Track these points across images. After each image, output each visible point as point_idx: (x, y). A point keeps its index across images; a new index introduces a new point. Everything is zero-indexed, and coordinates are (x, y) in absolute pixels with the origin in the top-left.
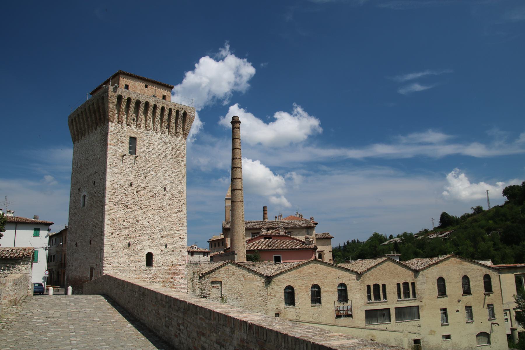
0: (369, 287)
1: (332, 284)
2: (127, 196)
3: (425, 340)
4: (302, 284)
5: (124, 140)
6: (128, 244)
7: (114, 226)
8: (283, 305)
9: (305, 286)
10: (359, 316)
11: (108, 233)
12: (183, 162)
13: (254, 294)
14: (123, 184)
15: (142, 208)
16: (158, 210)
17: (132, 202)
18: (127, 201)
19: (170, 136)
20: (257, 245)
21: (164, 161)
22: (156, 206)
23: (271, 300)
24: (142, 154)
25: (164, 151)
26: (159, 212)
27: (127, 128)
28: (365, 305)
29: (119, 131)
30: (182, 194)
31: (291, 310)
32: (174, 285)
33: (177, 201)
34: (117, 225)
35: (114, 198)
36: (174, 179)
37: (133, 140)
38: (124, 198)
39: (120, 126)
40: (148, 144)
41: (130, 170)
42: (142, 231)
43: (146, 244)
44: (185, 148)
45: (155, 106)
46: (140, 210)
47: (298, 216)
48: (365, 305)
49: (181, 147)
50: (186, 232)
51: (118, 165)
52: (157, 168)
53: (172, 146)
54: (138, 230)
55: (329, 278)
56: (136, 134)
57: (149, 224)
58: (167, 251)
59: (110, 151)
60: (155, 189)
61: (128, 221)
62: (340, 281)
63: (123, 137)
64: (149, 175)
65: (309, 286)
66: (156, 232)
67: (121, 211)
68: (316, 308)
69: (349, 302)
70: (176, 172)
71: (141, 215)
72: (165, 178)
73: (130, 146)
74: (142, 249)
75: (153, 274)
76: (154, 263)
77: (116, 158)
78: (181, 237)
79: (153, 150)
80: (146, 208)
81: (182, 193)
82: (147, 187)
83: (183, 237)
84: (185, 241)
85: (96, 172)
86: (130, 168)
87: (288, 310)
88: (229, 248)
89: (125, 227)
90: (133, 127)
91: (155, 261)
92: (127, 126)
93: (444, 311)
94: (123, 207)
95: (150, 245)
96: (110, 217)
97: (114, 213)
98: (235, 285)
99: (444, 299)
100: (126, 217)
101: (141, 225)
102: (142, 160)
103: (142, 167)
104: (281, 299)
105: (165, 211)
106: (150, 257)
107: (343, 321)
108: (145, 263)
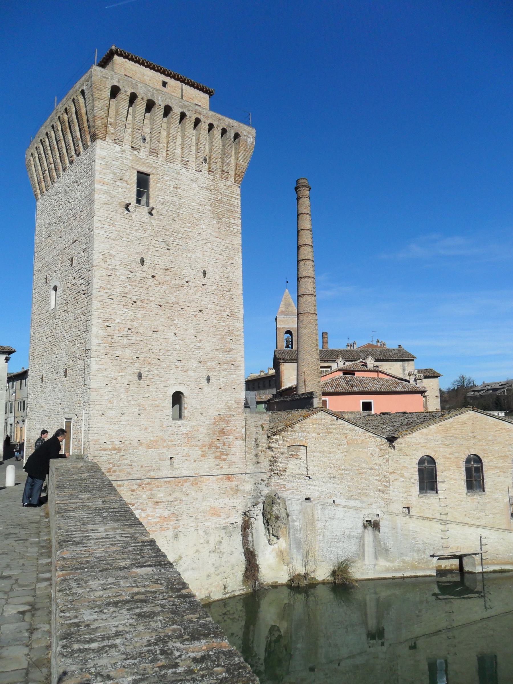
1: (503, 454)
2: (133, 284)
4: (450, 454)
5: (126, 178)
6: (137, 375)
7: (110, 339)
9: (455, 458)
11: (98, 353)
12: (234, 227)
13: (365, 470)
15: (163, 307)
16: (193, 313)
17: (144, 294)
18: (135, 293)
19: (211, 177)
20: (335, 384)
21: (201, 222)
22: (189, 304)
23: (395, 482)
24: (160, 206)
25: (200, 203)
26: (195, 316)
27: (131, 153)
29: (117, 159)
30: (234, 285)
31: (430, 498)
32: (222, 453)
33: (227, 298)
34: (115, 337)
35: (109, 286)
36: (220, 256)
38: (130, 287)
39: (118, 148)
40: (172, 189)
41: (140, 234)
42: (164, 351)
44: (239, 202)
46: (160, 311)
47: (379, 344)
49: (231, 199)
50: (243, 355)
51: (116, 223)
52: (189, 234)
53: (215, 197)
54: (155, 348)
55: (497, 443)
56: (149, 167)
57: (177, 338)
58: (210, 389)
59: (100, 196)
60: (187, 273)
61: (137, 331)
63: (124, 171)
64: (175, 247)
65: (462, 458)
66: (190, 353)
67: (123, 312)
68: (475, 499)
70: (223, 244)
71: (161, 320)
72: (205, 253)
73: (137, 190)
74: (164, 385)
75: (184, 432)
76: (185, 411)
77: (112, 210)
78: (233, 363)
79: (182, 200)
80: (170, 308)
82: (172, 269)
83: (237, 363)
85: (75, 239)
86: (140, 231)
87: (424, 501)
88: (290, 389)
89: (132, 342)
90: (143, 154)
91: (189, 408)
92: (132, 151)
94: (126, 304)
95: (178, 377)
96: (101, 321)
97: (109, 316)
98: (330, 452)
100: (132, 323)
101: (161, 340)
102: (161, 217)
103: (162, 230)
104: (413, 481)
105: (205, 314)
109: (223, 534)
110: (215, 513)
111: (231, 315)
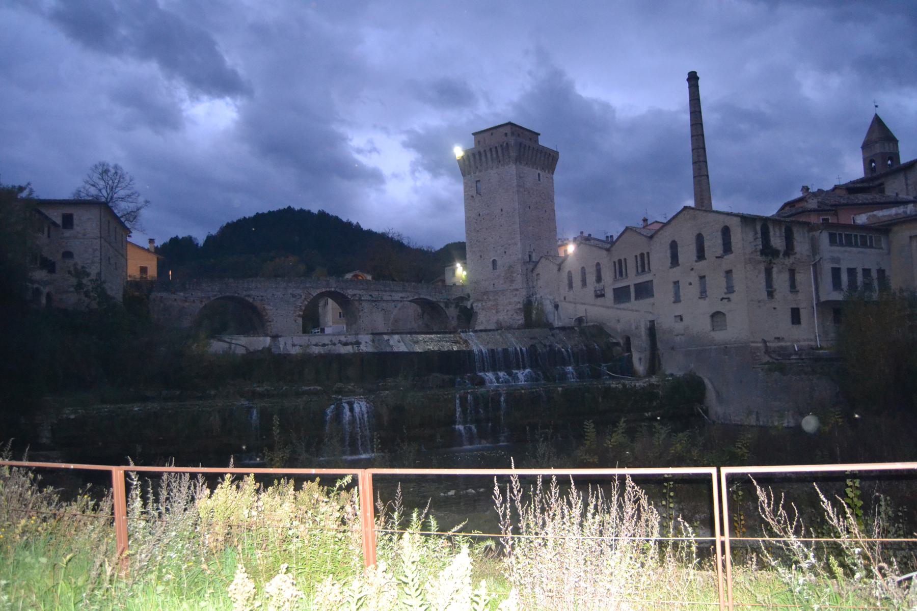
0: (615, 262)
3: (659, 322)
10: (610, 294)
31: (571, 292)
39: (469, 176)
45: (485, 151)
69: (603, 281)
84: (519, 244)
106: (494, 262)
107: (600, 301)
108: (492, 268)
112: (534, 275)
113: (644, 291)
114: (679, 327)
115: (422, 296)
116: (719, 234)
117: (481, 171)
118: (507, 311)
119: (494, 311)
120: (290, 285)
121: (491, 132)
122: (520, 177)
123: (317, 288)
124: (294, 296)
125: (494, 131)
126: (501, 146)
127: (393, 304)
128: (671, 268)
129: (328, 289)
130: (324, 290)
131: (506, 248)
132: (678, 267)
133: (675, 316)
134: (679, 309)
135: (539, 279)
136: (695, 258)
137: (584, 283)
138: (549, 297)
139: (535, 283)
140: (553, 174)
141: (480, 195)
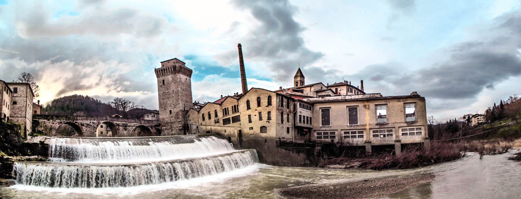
0: (223, 109)
3: (243, 130)
8: (202, 121)
14: (162, 93)
28: (223, 117)
31: (204, 122)
37: (163, 81)
43: (169, 108)
45: (166, 69)
48: (223, 117)
62: (215, 109)
81: (178, 90)
93: (249, 116)
99: (250, 110)
106: (171, 111)
107: (217, 124)
108: (169, 113)
109: (179, 130)
110: (177, 127)
111: (179, 96)
112: (187, 116)
113: (236, 119)
114: (251, 132)
115: (142, 124)
116: (267, 98)
117: (164, 76)
118: (176, 130)
119: (171, 130)
120: (92, 119)
121: (168, 62)
122: (180, 79)
123: (103, 120)
124: (93, 123)
125: (169, 61)
126: (173, 67)
127: (131, 127)
128: (247, 110)
129: (107, 121)
130: (105, 121)
131: (175, 105)
132: (250, 110)
133: (250, 128)
134: (251, 125)
135: (189, 117)
136: (257, 106)
137: (210, 118)
138: (194, 124)
139: (188, 119)
140: (190, 78)
141: (164, 85)
